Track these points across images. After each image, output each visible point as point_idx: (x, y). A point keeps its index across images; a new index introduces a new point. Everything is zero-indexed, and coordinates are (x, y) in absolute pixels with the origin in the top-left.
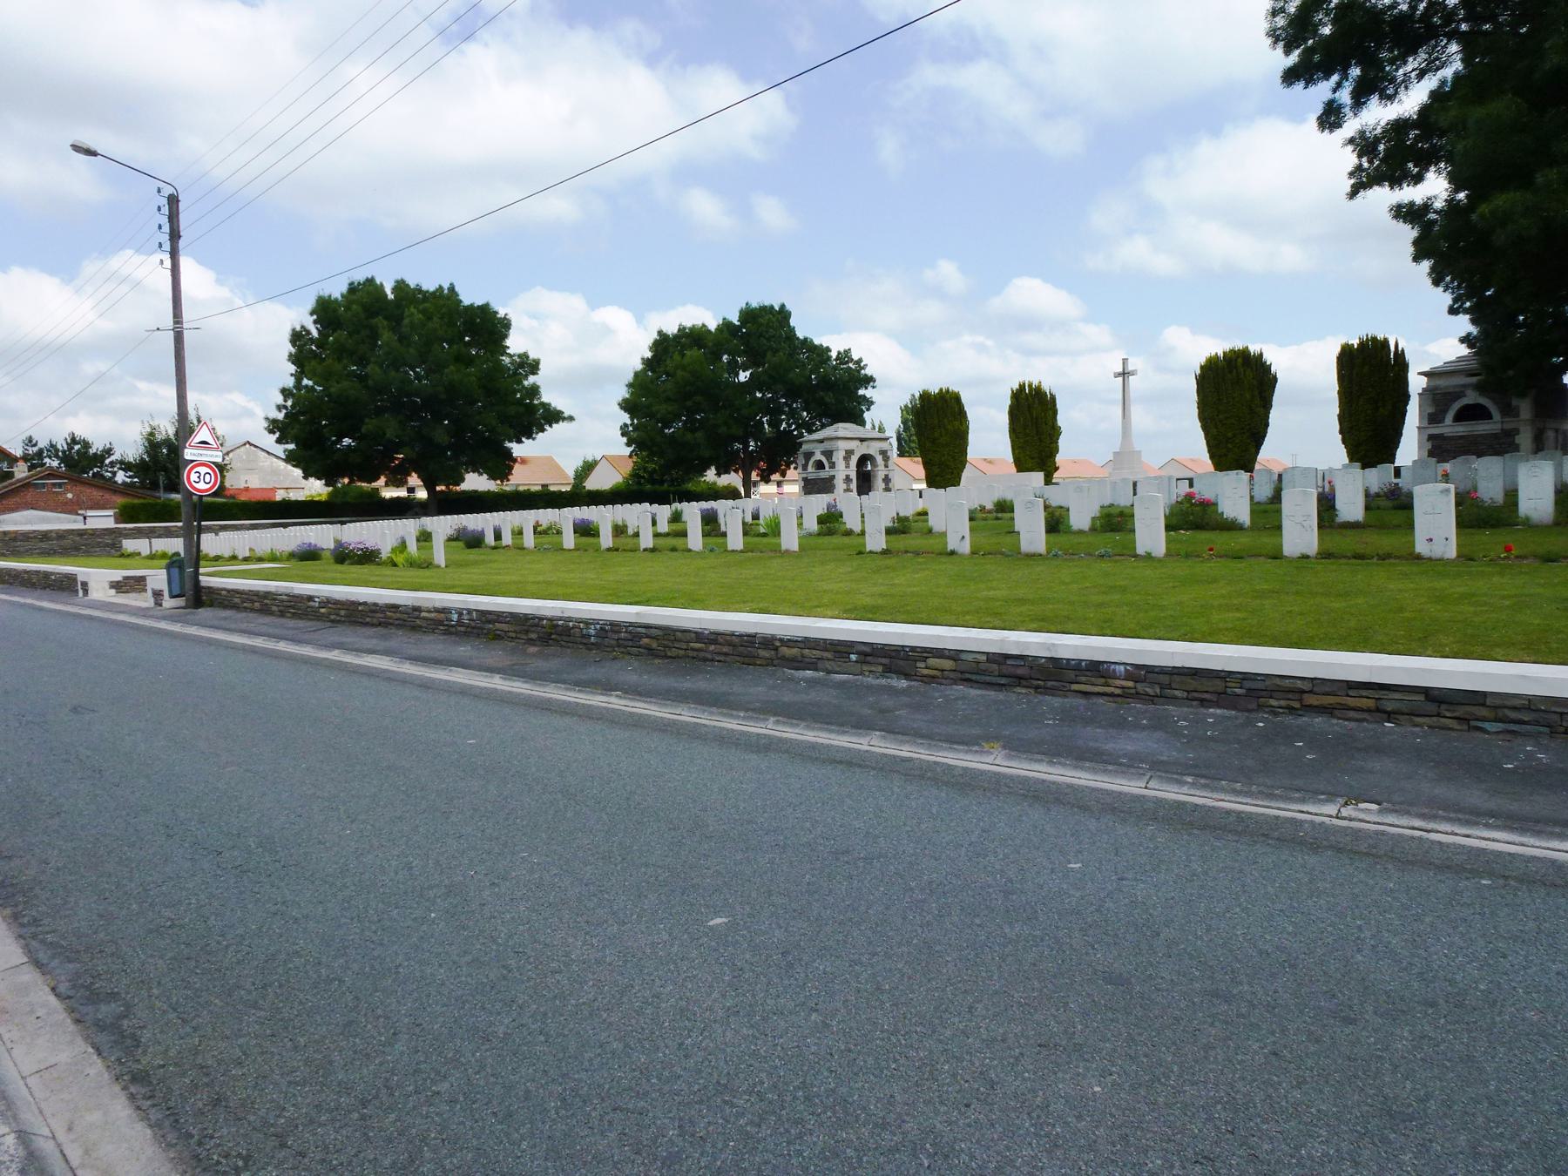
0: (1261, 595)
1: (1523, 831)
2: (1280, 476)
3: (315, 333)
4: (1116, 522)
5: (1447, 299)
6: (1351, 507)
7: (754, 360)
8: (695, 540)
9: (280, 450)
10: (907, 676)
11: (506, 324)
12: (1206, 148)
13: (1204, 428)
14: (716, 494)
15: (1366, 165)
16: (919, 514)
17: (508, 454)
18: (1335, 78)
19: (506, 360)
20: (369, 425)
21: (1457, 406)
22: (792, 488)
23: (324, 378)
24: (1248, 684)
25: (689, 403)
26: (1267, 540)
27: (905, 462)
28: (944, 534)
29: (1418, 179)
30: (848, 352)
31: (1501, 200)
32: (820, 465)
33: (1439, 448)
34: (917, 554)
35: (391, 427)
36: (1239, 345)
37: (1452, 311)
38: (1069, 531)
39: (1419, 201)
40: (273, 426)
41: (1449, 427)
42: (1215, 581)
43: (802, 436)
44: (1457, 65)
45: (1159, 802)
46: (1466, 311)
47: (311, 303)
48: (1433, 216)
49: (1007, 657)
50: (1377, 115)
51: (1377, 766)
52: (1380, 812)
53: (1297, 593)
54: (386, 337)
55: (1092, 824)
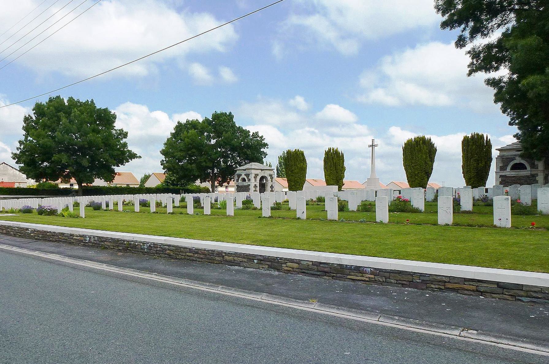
0: (429, 240)
1: (538, 344)
2: (437, 190)
3: (34, 118)
4: (368, 208)
5: (508, 119)
6: (467, 205)
7: (218, 134)
8: (190, 209)
9: (17, 166)
10: (278, 270)
11: (114, 117)
12: (408, 53)
13: (406, 169)
14: (199, 190)
15: (475, 62)
16: (285, 202)
17: (113, 171)
18: (463, 26)
19: (114, 132)
20: (55, 157)
21: (512, 163)
22: (232, 189)
23: (37, 137)
24: (422, 278)
25: (190, 152)
26: (431, 217)
27: (280, 179)
28: (295, 210)
29: (497, 69)
30: (257, 133)
31: (531, 79)
32: (244, 180)
33: (505, 181)
34: (284, 218)
35: (64, 158)
36: (421, 135)
37: (510, 124)
38: (348, 211)
39: (497, 78)
40: (15, 156)
41: (508, 172)
42: (409, 234)
43: (237, 167)
44: (513, 23)
45: (384, 327)
46: (516, 124)
47: (33, 107)
48: (503, 84)
49: (321, 263)
50: (480, 42)
51: (477, 315)
52: (477, 334)
53: (444, 240)
54: (64, 120)
55: (355, 336)
